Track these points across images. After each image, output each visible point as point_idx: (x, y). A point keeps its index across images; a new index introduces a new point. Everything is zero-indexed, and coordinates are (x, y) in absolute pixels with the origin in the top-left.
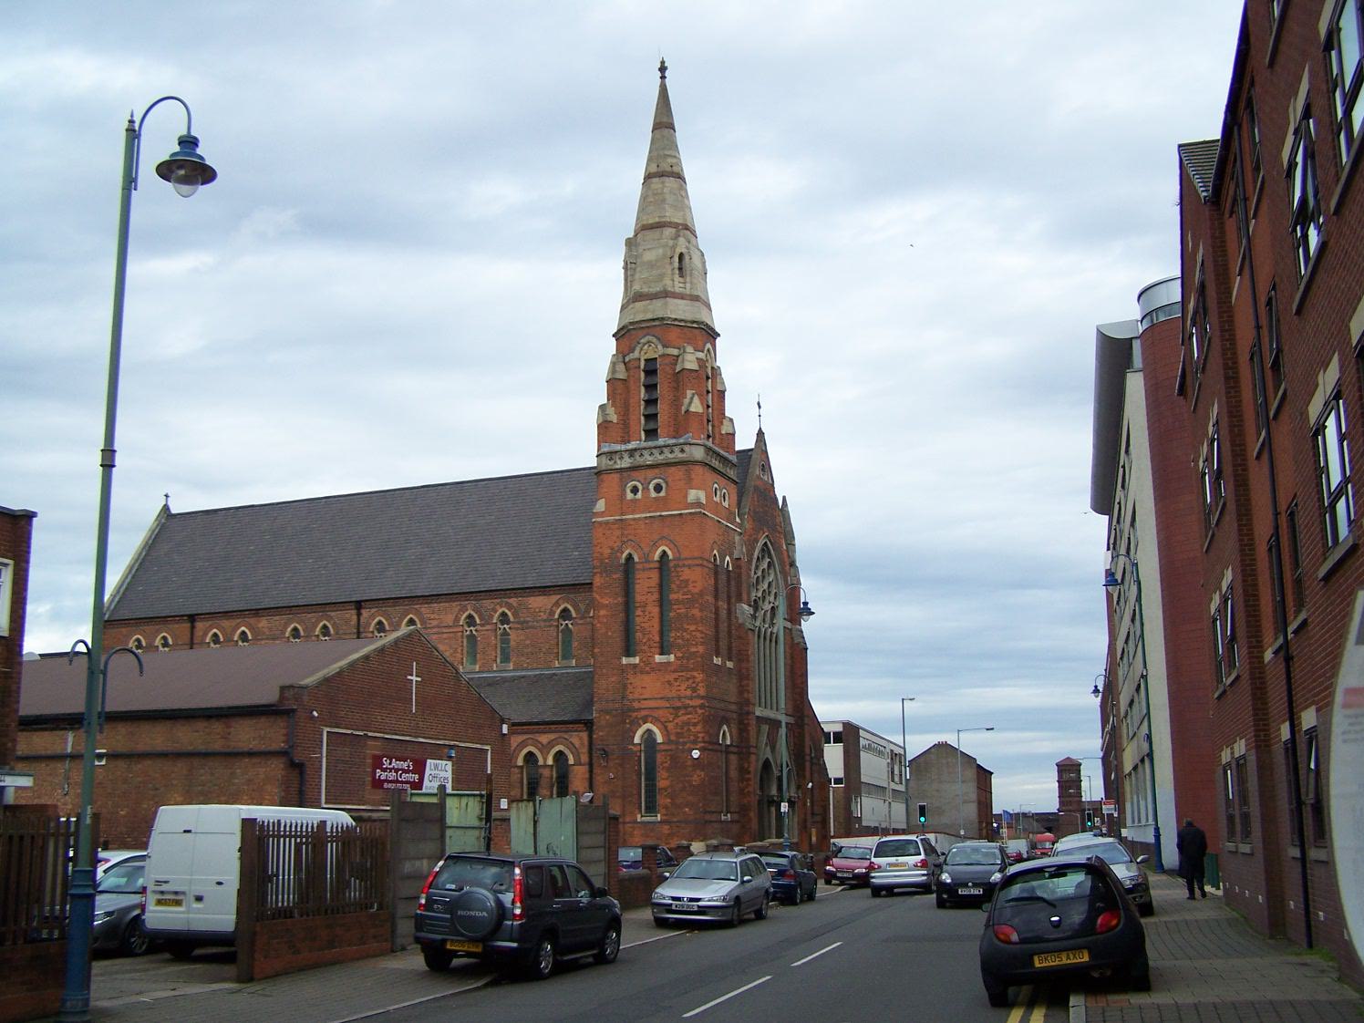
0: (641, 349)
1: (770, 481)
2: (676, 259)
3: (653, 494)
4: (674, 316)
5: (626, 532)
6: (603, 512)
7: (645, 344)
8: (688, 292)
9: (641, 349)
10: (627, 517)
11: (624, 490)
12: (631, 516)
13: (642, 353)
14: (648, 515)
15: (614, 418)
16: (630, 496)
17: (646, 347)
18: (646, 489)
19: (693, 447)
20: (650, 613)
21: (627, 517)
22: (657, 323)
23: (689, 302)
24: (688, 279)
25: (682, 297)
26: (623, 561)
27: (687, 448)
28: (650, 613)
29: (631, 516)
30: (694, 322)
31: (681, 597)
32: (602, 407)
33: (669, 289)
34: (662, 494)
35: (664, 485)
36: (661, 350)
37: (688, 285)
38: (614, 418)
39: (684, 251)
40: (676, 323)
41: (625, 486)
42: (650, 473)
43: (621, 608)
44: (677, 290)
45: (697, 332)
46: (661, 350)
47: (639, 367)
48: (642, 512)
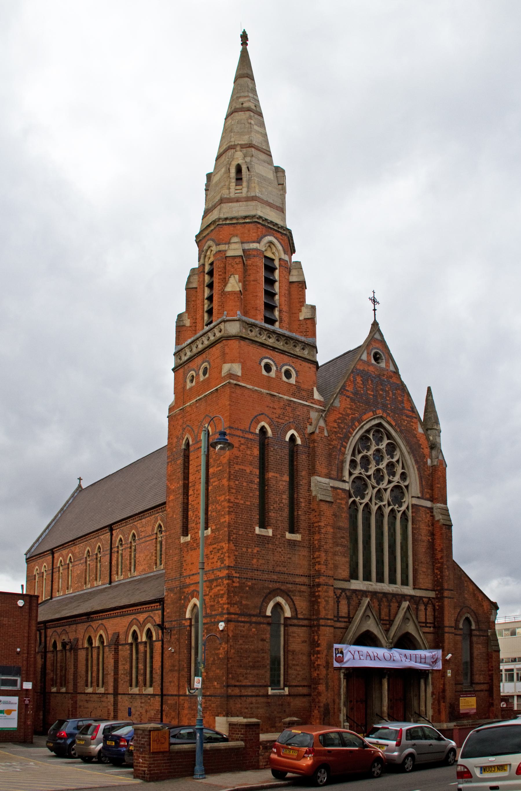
0: (205, 256)
1: (392, 368)
2: (233, 171)
3: (202, 378)
4: (225, 217)
5: (185, 419)
6: (174, 406)
7: (207, 251)
8: (244, 195)
9: (205, 256)
10: (186, 405)
11: (186, 382)
12: (189, 404)
13: (207, 260)
14: (198, 398)
15: (187, 322)
16: (189, 385)
17: (208, 253)
18: (198, 375)
19: (228, 324)
20: (197, 491)
21: (186, 405)
22: (212, 227)
23: (244, 203)
24: (245, 184)
25: (238, 200)
26: (183, 447)
27: (222, 326)
28: (197, 491)
29: (189, 404)
30: (246, 217)
31: (216, 470)
32: (180, 316)
33: (225, 196)
34: (207, 376)
35: (208, 367)
36: (214, 249)
37: (245, 190)
38: (187, 322)
39: (240, 162)
40: (228, 222)
41: (186, 378)
42: (198, 360)
43: (181, 491)
44: (232, 195)
45: (251, 225)
46: (214, 249)
47: (204, 272)
48: (195, 398)
